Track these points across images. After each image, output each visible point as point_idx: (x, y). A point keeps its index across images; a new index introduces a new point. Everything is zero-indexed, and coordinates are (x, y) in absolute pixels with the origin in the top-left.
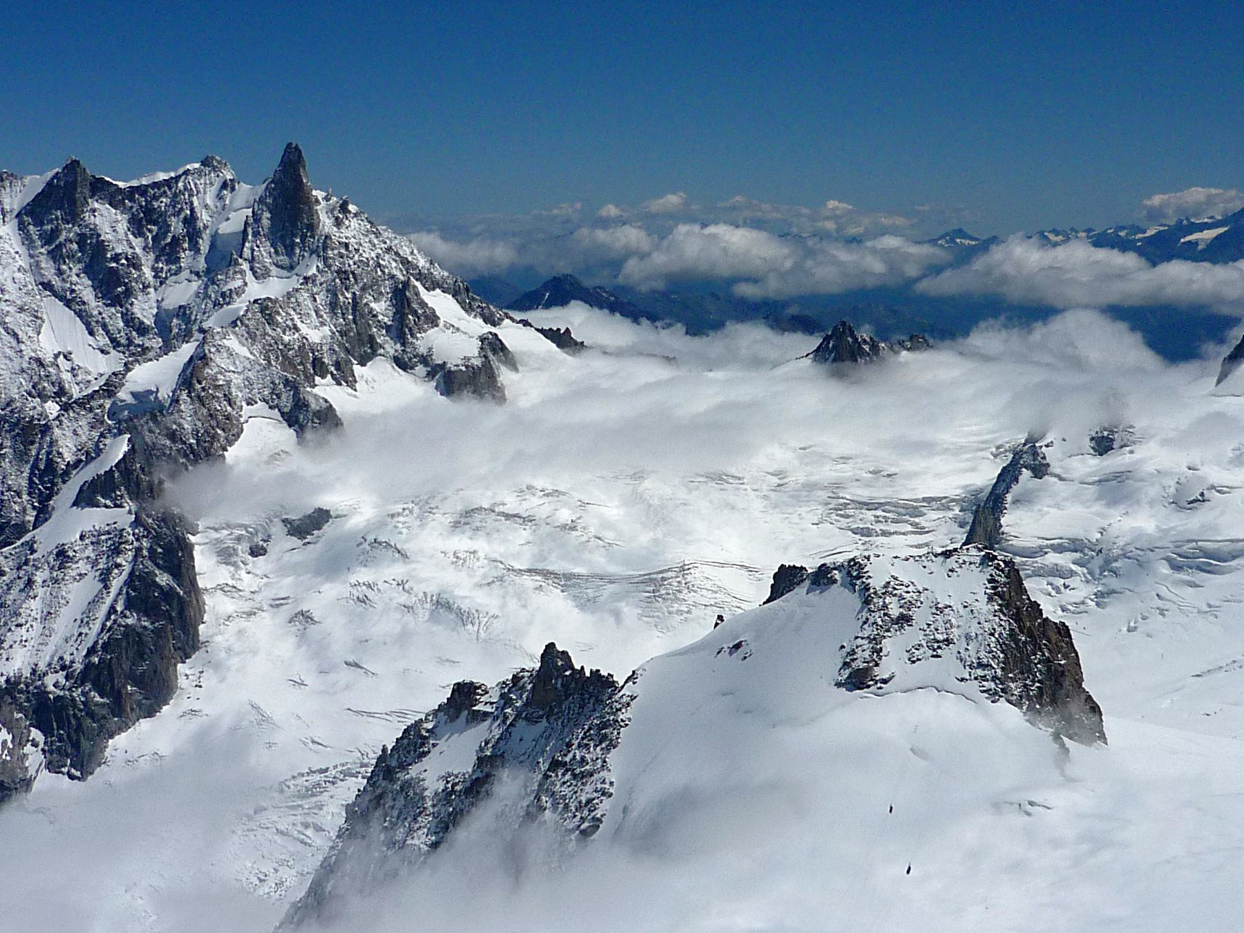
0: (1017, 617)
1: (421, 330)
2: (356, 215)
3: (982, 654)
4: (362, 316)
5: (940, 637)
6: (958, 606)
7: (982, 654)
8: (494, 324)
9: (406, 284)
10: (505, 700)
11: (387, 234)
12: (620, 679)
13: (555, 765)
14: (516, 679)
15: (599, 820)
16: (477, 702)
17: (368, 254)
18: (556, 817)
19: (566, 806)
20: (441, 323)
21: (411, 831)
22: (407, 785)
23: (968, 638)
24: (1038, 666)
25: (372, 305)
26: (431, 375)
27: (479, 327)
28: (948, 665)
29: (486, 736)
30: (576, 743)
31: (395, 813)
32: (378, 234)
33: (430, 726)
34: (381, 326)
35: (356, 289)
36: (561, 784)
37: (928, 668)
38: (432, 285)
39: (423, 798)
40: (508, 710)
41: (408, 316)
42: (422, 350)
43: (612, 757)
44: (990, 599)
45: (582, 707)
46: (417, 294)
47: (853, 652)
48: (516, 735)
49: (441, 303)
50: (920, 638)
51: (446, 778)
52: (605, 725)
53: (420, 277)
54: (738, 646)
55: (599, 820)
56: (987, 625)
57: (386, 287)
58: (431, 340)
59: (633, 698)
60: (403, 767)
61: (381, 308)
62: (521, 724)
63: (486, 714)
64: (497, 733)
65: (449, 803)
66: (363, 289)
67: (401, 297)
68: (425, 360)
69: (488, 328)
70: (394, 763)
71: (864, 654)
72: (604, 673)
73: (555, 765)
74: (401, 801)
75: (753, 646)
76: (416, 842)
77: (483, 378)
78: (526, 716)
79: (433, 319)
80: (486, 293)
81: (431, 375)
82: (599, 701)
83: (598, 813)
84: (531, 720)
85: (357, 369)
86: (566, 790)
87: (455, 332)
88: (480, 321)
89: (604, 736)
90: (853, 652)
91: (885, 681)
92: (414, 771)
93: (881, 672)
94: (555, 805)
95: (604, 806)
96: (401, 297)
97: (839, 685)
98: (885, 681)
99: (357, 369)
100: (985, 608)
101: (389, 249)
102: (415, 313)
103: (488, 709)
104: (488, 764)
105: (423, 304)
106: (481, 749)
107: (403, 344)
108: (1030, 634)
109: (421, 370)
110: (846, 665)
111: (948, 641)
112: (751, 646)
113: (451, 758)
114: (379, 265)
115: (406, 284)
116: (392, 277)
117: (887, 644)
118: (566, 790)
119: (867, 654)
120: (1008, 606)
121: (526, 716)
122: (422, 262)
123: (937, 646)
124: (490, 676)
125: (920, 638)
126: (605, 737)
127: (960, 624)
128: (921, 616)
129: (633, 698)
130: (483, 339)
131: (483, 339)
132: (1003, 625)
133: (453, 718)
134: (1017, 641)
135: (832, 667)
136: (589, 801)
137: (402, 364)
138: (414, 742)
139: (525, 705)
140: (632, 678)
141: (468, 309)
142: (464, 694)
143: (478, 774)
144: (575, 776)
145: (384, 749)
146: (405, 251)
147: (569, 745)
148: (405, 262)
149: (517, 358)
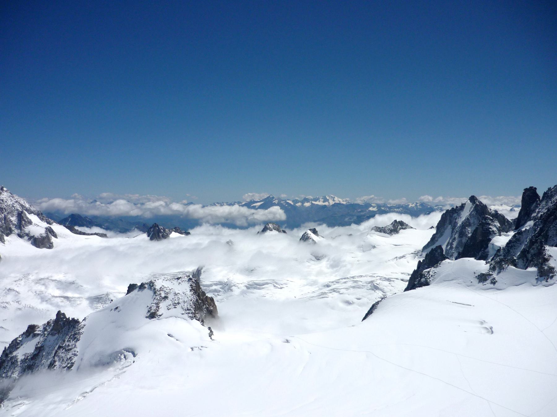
0: (199, 296)
1: (27, 226)
2: (6, 191)
3: (189, 306)
4: (7, 221)
5: (176, 302)
6: (181, 293)
7: (189, 306)
8: (50, 224)
9: (22, 212)
10: (45, 329)
11: (16, 197)
12: (81, 320)
13: (60, 347)
14: (48, 323)
15: (73, 363)
16: (36, 330)
17: (10, 203)
18: (60, 363)
19: (63, 360)
20: (33, 224)
21: (13, 373)
22: (12, 358)
23: (184, 302)
24: (203, 306)
25: (11, 218)
26: (29, 239)
27: (45, 225)
28: (179, 310)
29: (38, 341)
30: (66, 340)
31: (8, 367)
32: (13, 197)
33: (20, 339)
34: (13, 225)
35: (6, 213)
36: (61, 353)
37: (173, 311)
38: (31, 212)
39: (17, 362)
40: (46, 332)
41: (22, 221)
42: (27, 231)
43: (78, 344)
44: (191, 291)
45: (69, 330)
46: (25, 215)
47: (151, 308)
48: (48, 340)
49: (33, 218)
50: (171, 303)
51: (25, 355)
52: (75, 334)
53: (27, 210)
54: (117, 308)
55: (73, 363)
56: (190, 298)
57: (15, 213)
58: (29, 229)
59: (84, 325)
60: (11, 353)
61: (14, 219)
62: (50, 336)
63: (38, 334)
64: (42, 339)
65: (26, 363)
66: (8, 213)
67: (20, 216)
68: (27, 235)
69: (48, 225)
70: (8, 352)
71: (154, 308)
72: (76, 319)
73: (60, 347)
74: (10, 364)
75: (121, 308)
76: (14, 376)
77: (46, 240)
78: (52, 334)
79: (30, 223)
80: (48, 216)
81: (29, 239)
82: (74, 327)
83: (73, 361)
84: (53, 335)
85: (6, 238)
86: (63, 355)
87: (38, 226)
88: (46, 223)
89: (75, 338)
90: (151, 308)
91: (160, 316)
92: (14, 354)
93: (159, 313)
94: (59, 360)
95: (75, 359)
96: (20, 216)
97: (147, 317)
98: (160, 316)
99: (6, 238)
100: (189, 293)
101: (16, 202)
102: (24, 221)
103: (39, 332)
104: (39, 350)
105: (27, 218)
106: (37, 345)
107: (21, 230)
108: (202, 300)
109: (26, 238)
110: (149, 311)
111: (179, 303)
112: (121, 308)
113: (27, 349)
114: (13, 206)
115: (22, 212)
116: (17, 210)
117: (161, 305)
118: (63, 355)
119: (155, 308)
120: (196, 293)
121: (52, 334)
122: (27, 206)
123: (175, 305)
124: (40, 323)
125: (171, 303)
126: (76, 338)
127: (182, 298)
128: (171, 296)
129: (84, 325)
130: (46, 228)
131: (46, 228)
132: (194, 298)
133: (28, 336)
134: (198, 302)
135: (145, 312)
136: (70, 358)
137: (20, 236)
138: (15, 345)
139: (52, 330)
140: (84, 320)
141: (42, 219)
142: (31, 329)
143: (36, 353)
144: (66, 350)
145: (5, 348)
146: (22, 202)
147: (64, 341)
148: (22, 206)
149: (57, 234)
